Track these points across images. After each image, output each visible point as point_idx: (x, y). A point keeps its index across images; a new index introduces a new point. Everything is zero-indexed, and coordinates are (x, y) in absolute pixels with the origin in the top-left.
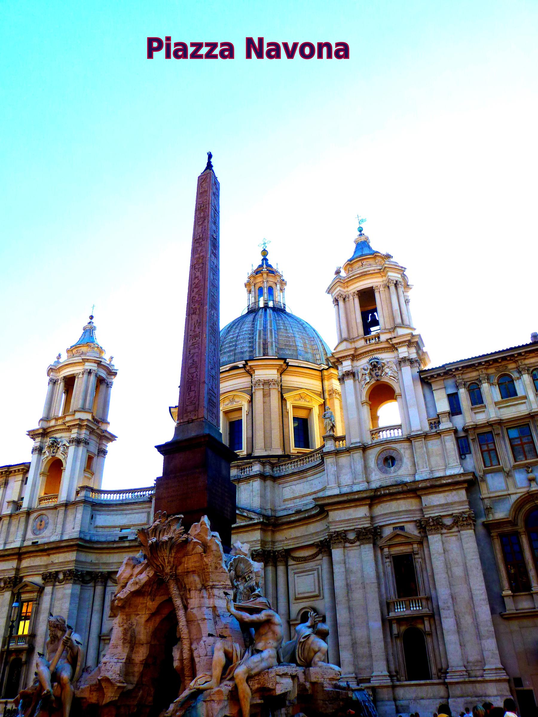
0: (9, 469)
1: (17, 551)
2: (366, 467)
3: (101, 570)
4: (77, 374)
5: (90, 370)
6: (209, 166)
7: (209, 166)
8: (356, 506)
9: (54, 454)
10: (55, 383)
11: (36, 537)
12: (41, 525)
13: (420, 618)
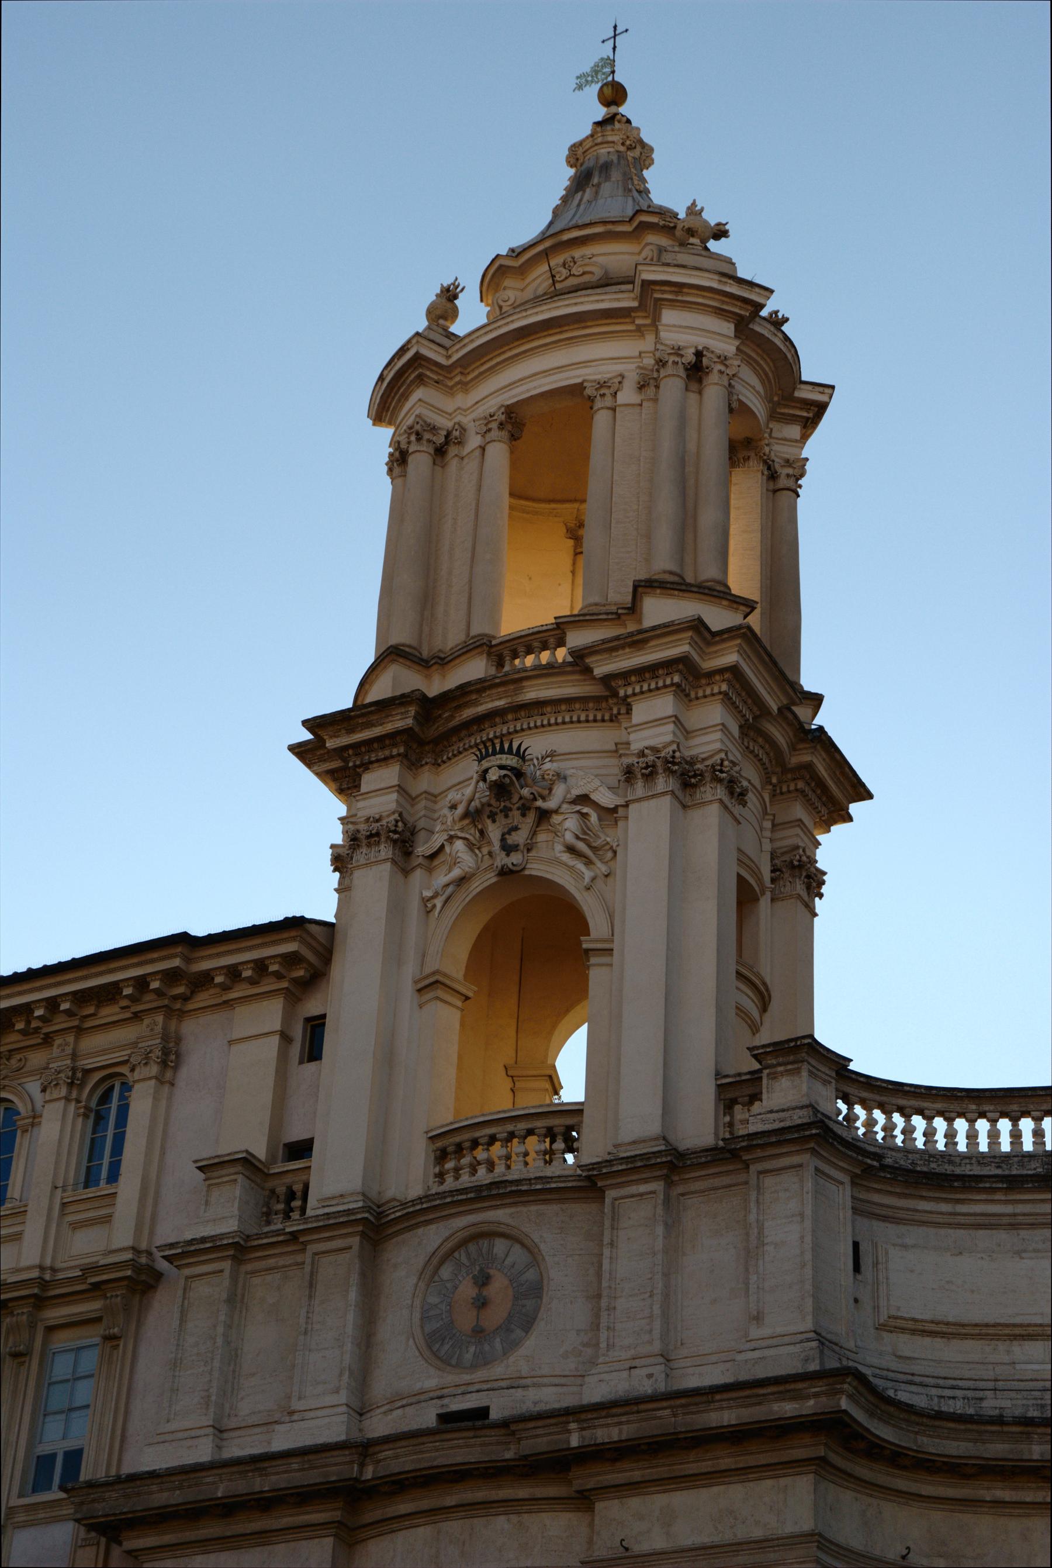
0: (188, 960)
1: (337, 1469)
4: (602, 385)
5: (699, 354)
9: (516, 858)
10: (440, 452)
11: (466, 1378)
12: (481, 1304)
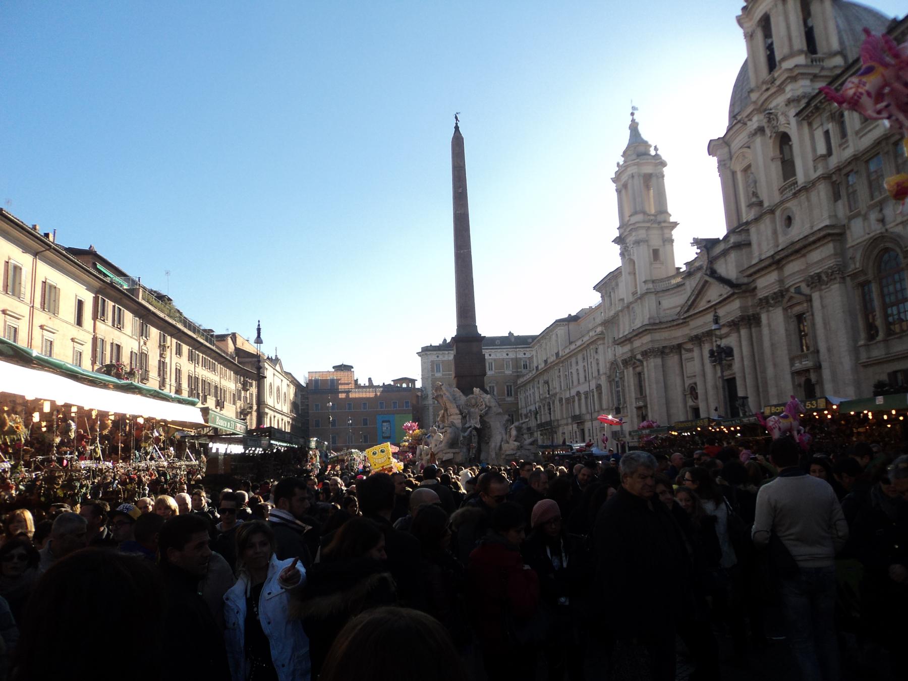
2: (775, 232)
3: (673, 344)
6: (457, 128)
7: (457, 128)
8: (769, 272)
13: (807, 371)
